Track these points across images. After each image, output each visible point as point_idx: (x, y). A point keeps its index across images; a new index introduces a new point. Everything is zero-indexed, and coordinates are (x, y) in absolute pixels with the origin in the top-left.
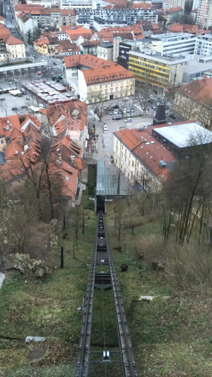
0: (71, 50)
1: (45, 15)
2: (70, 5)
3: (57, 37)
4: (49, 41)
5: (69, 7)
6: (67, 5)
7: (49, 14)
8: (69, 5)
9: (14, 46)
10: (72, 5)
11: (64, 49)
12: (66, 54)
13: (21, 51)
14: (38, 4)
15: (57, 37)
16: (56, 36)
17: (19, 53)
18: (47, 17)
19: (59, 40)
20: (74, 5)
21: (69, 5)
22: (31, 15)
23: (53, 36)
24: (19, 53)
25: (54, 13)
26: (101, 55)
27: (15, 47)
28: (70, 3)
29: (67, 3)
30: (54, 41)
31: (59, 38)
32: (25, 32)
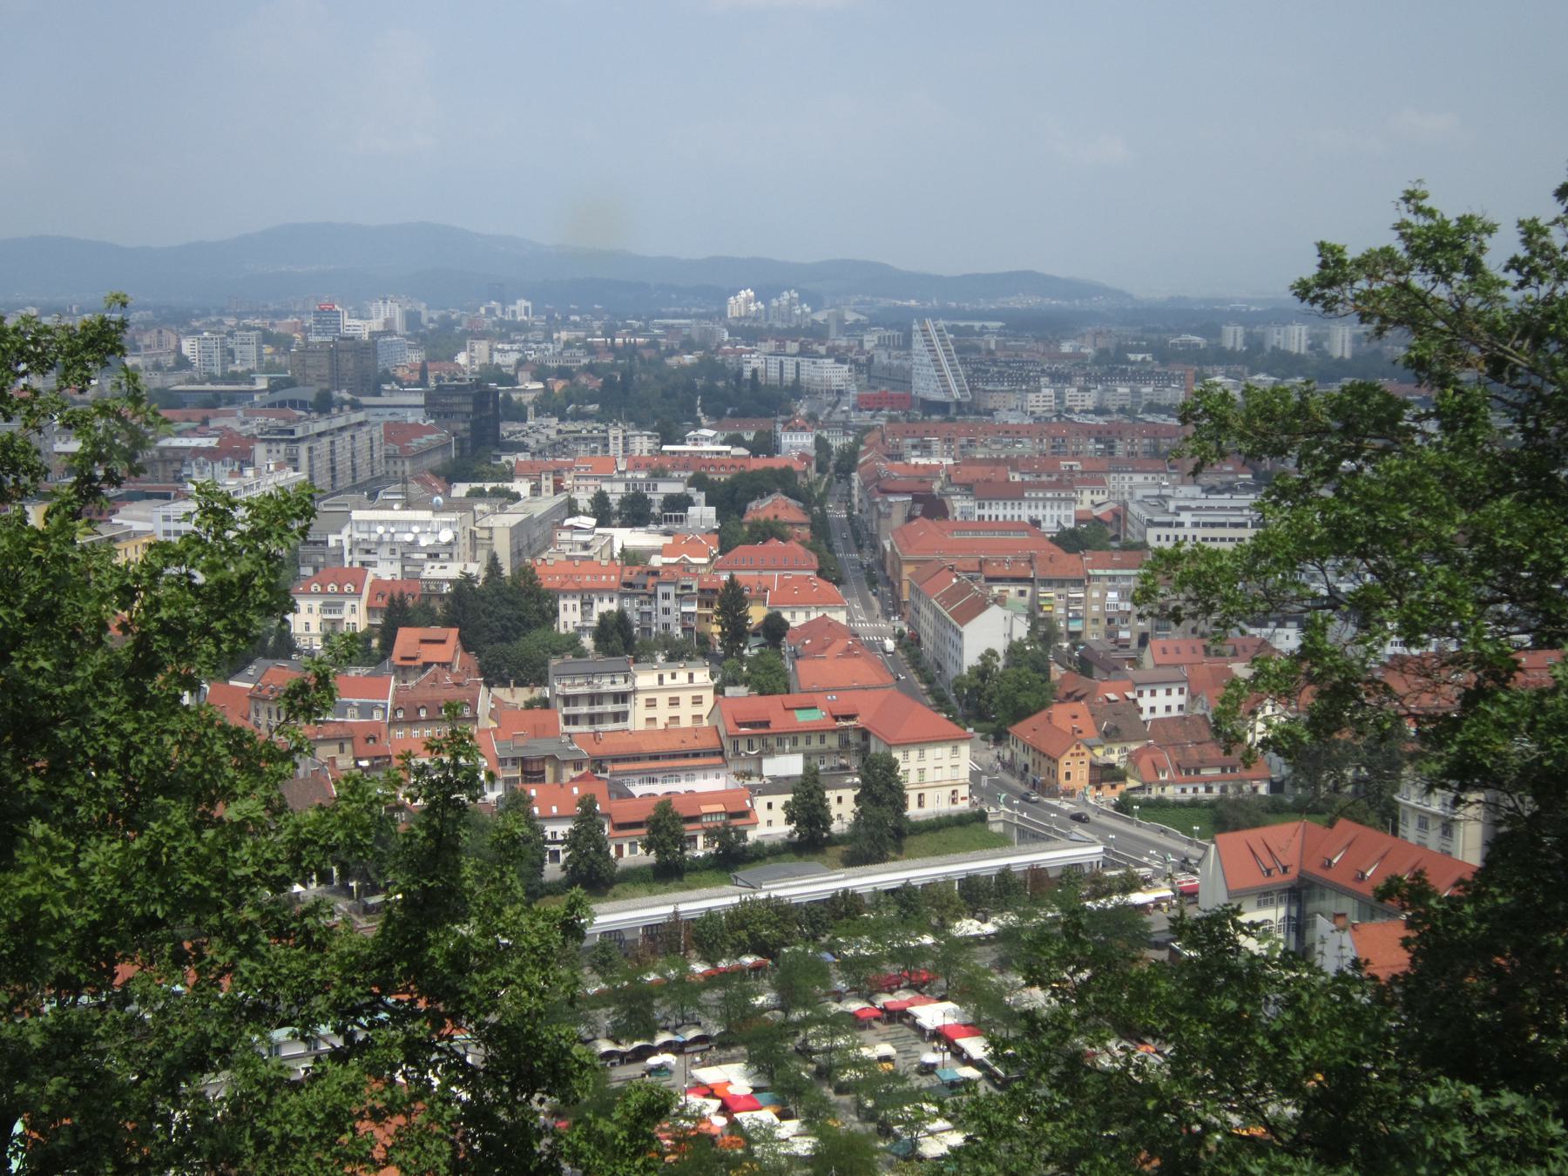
0: (1217, 771)
1: (1062, 583)
2: (1188, 525)
3: (1135, 701)
4: (1098, 725)
5: (1180, 532)
6: (1169, 525)
7: (1082, 576)
8: (1180, 525)
9: (914, 754)
10: (1196, 525)
11: (1178, 767)
12: (1190, 791)
13: (946, 774)
14: (1009, 512)
15: (1135, 701)
16: (1131, 695)
17: (938, 785)
18: (1072, 589)
19: (1146, 715)
20: (1205, 525)
21: (1180, 525)
22: (988, 579)
23: (1112, 696)
24: (938, 785)
25: (1109, 572)
26: (1423, 824)
27: (922, 755)
28: (1186, 518)
29: (1166, 512)
30: (1119, 723)
31: (1145, 702)
32: (952, 672)
